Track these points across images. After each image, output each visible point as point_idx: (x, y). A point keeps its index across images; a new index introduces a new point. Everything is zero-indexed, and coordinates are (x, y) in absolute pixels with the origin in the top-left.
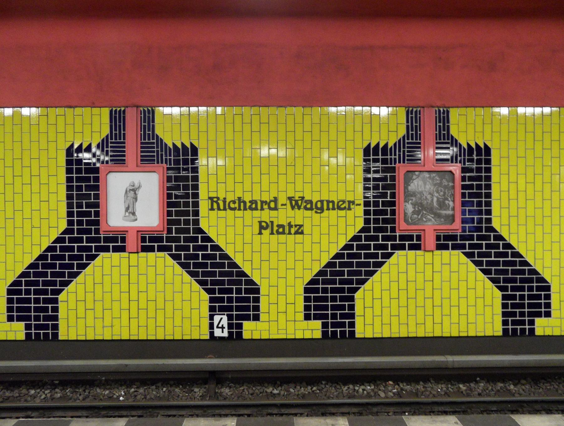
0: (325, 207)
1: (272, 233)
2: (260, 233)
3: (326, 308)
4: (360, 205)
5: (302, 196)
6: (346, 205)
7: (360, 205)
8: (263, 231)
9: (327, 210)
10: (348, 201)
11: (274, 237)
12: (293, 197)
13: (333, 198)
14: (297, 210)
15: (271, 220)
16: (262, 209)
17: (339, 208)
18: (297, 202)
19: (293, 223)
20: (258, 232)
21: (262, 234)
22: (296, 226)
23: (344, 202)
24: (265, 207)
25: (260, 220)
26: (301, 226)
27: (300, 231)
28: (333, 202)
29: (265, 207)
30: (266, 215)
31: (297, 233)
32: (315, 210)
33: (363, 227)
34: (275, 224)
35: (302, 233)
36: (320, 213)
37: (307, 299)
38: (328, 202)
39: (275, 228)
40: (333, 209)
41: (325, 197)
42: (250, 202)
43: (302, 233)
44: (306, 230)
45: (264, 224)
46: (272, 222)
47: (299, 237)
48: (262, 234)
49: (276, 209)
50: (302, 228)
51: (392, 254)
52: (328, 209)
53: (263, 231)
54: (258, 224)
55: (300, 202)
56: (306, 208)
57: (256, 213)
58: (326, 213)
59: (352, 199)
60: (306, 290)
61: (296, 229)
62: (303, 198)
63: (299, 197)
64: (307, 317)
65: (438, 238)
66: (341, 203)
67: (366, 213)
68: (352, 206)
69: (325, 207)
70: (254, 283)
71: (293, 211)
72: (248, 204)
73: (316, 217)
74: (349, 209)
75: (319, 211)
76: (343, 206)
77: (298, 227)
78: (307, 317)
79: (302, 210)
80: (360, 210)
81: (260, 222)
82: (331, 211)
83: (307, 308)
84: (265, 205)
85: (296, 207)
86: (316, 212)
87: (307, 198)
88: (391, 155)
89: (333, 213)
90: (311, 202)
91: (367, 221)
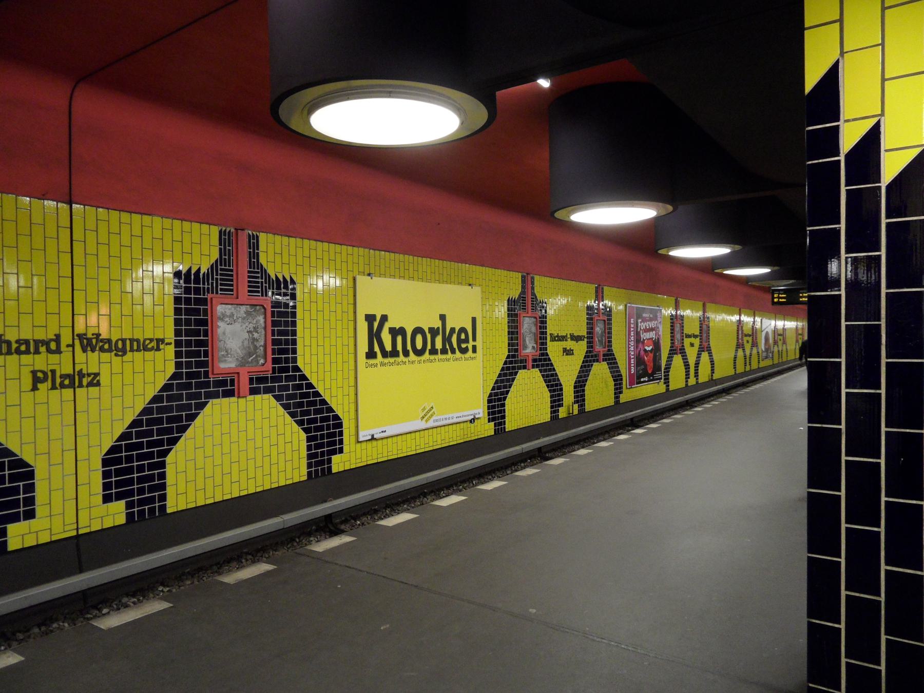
0: (128, 348)
1: (54, 387)
2: (35, 388)
3: (130, 482)
4: (170, 344)
5: (96, 332)
6: (154, 344)
7: (170, 344)
8: (39, 386)
9: (130, 351)
10: (156, 339)
11: (56, 393)
12: (85, 334)
13: (138, 335)
14: (89, 353)
15: (51, 367)
16: (37, 352)
17: (146, 349)
18: (89, 340)
19: (85, 371)
20: (30, 387)
21: (38, 389)
22: (89, 375)
23: (151, 340)
24: (43, 349)
25: (32, 369)
26: (97, 375)
27: (95, 382)
28: (138, 341)
29: (43, 349)
30: (41, 361)
31: (90, 384)
32: (115, 352)
33: (175, 373)
34: (58, 375)
35: (98, 384)
36: (122, 356)
37: (106, 475)
38: (132, 340)
39: (58, 380)
40: (138, 350)
41: (127, 335)
42: (17, 342)
43: (98, 384)
44: (104, 379)
45: (40, 375)
46: (53, 372)
47: (93, 390)
48: (38, 389)
49: (58, 351)
50: (98, 378)
51: (205, 404)
52: (132, 350)
53: (39, 386)
54: (30, 376)
55: (94, 341)
56: (102, 350)
57: (26, 359)
58: (129, 354)
59: (162, 337)
60: (105, 463)
61: (90, 379)
62: (98, 335)
63: (93, 335)
64: (107, 499)
65: (251, 380)
66: (147, 342)
67: (178, 354)
68: (162, 347)
69: (128, 348)
70: (25, 464)
71: (85, 354)
72: (14, 346)
73: (117, 361)
74: (158, 349)
75: (120, 353)
76: (150, 346)
77: (92, 376)
78: (107, 499)
79: (97, 353)
80: (170, 351)
81: (34, 373)
82: (135, 353)
83: (106, 486)
84: (42, 346)
85: (89, 349)
86: (116, 355)
87: (104, 335)
88: (204, 284)
89: (138, 356)
90: (109, 341)
91: (178, 365)
